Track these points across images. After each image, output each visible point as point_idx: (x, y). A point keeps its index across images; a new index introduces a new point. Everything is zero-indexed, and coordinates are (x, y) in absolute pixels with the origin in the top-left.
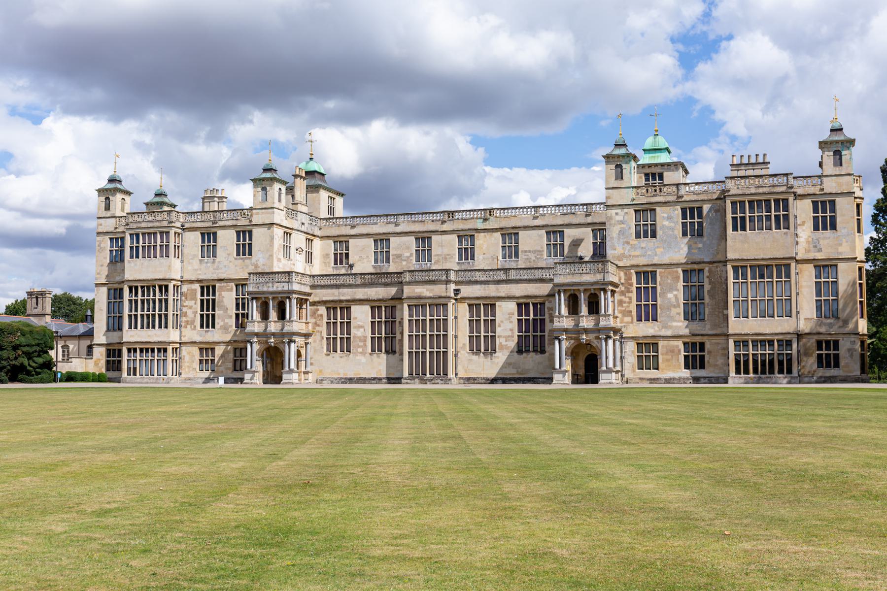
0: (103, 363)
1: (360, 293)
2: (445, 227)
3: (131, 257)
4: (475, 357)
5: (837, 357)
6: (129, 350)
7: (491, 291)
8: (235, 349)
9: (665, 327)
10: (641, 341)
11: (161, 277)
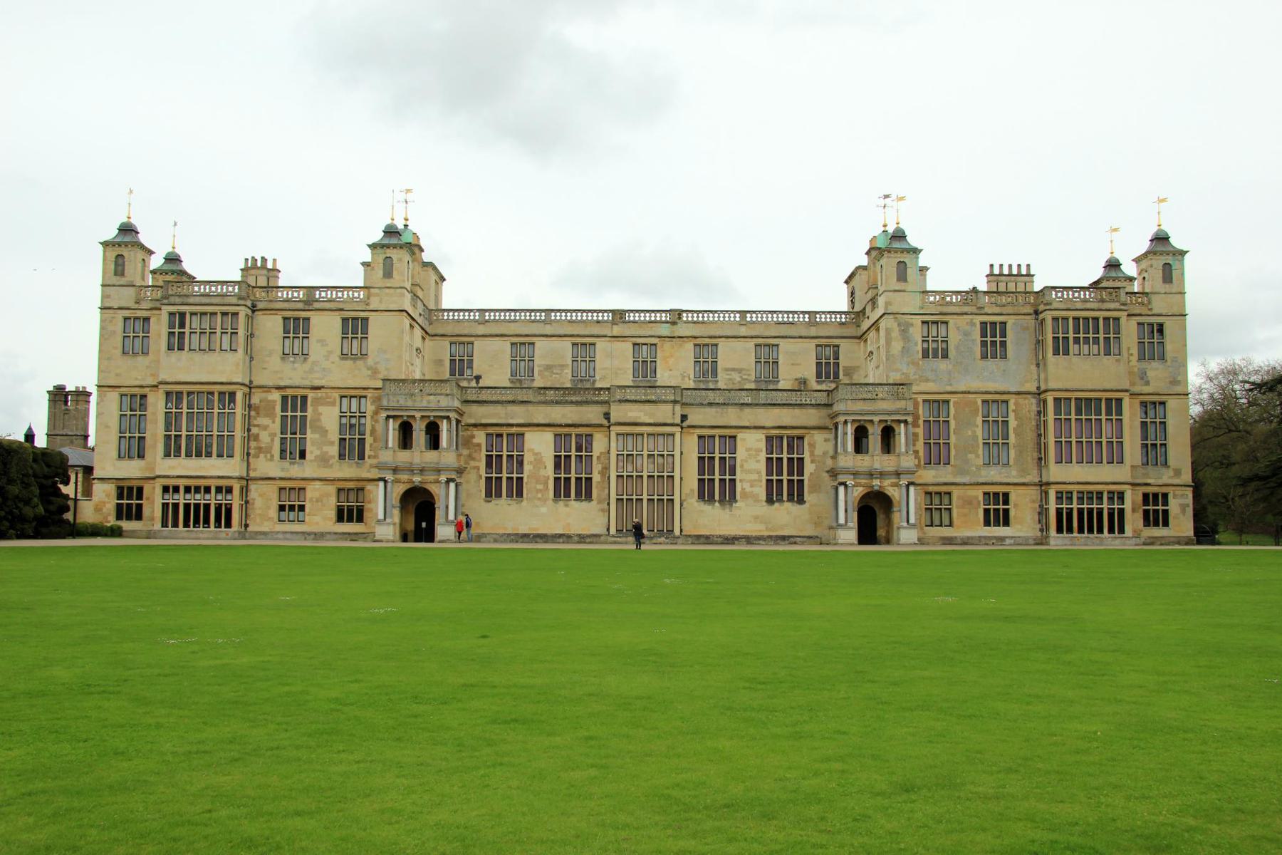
0: (111, 505)
2: (617, 330)
4: (707, 508)
5: (1166, 513)
6: (166, 489)
7: (731, 417)
8: (339, 490)
9: (962, 472)
10: (931, 489)
11: (224, 380)
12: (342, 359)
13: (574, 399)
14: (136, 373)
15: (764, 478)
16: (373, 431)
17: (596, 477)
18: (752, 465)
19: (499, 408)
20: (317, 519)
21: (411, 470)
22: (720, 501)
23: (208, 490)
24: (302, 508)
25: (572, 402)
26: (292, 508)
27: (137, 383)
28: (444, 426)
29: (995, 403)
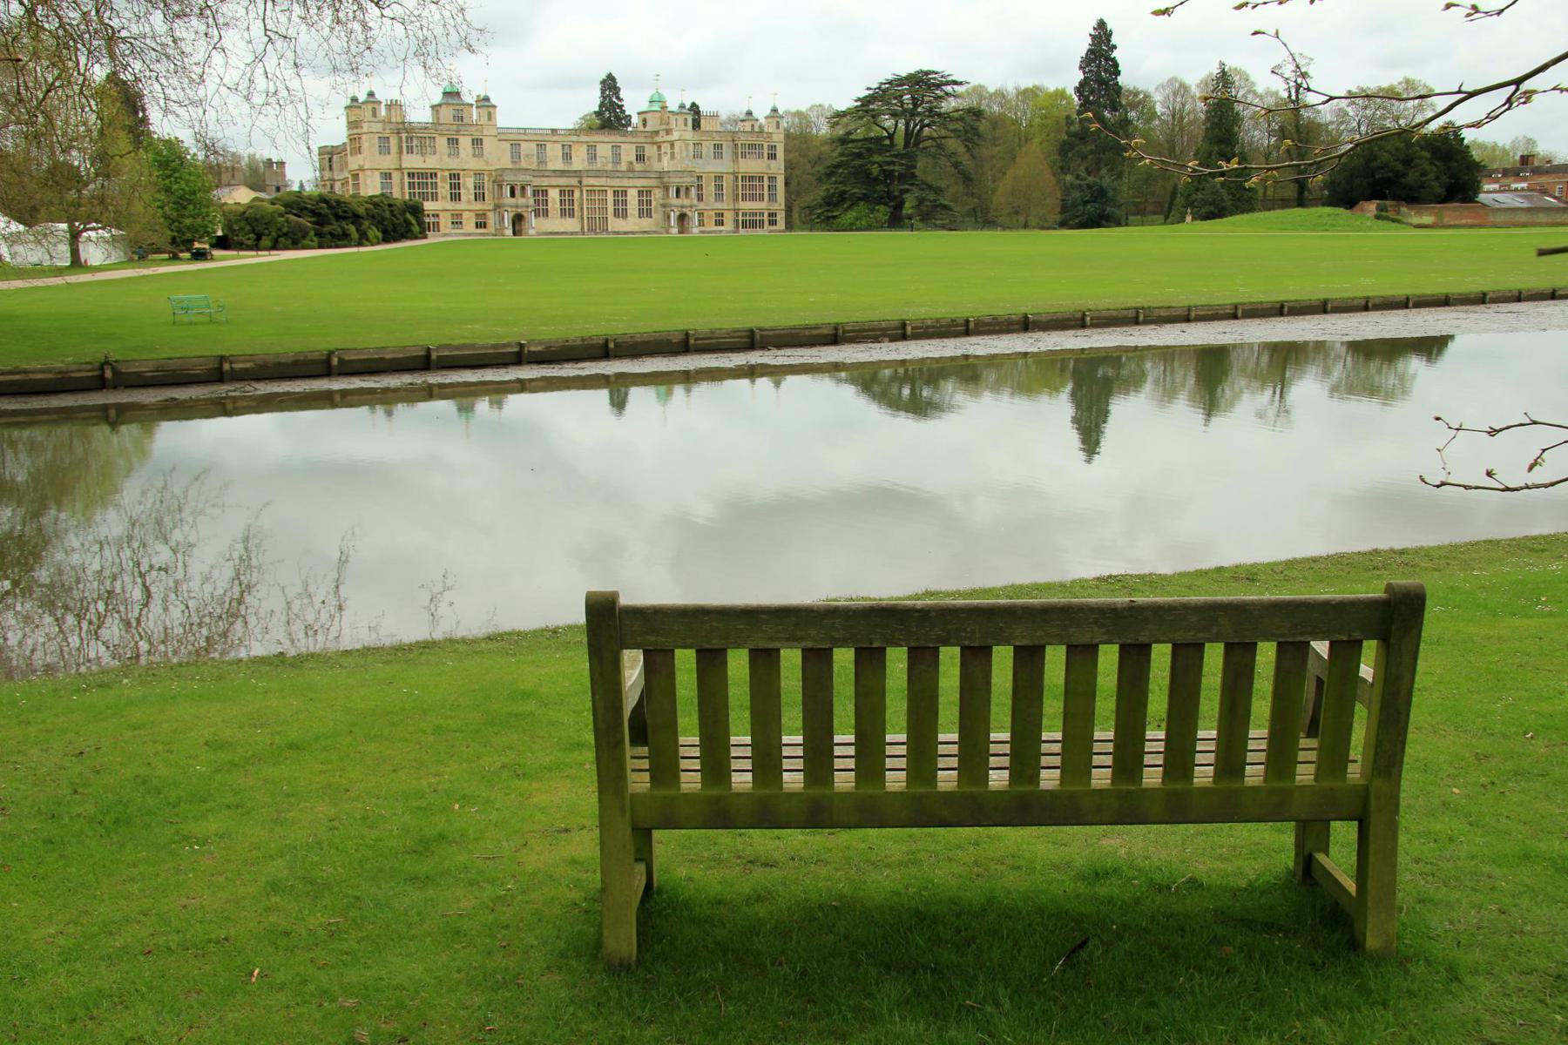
1: (555, 181)
7: (626, 183)
14: (388, 162)
29: (719, 178)
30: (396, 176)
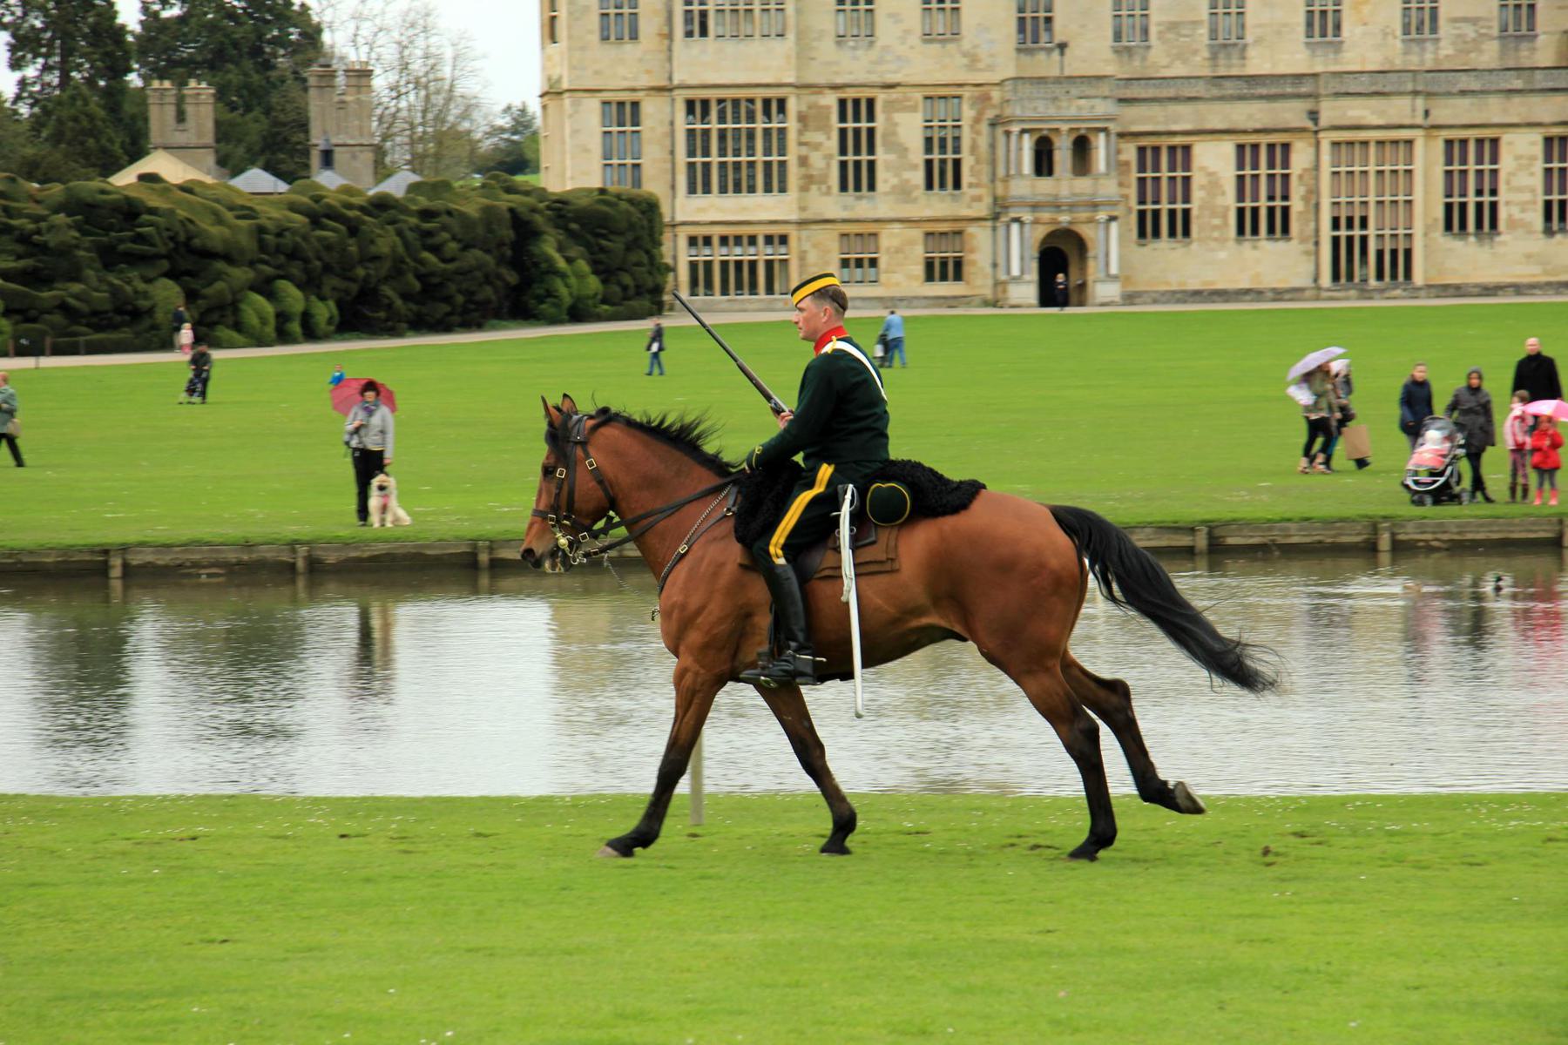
1: (1217, 115)
3: (689, 34)
4: (1456, 244)
6: (693, 241)
7: (1494, 110)
8: (928, 234)
12: (926, 42)
13: (1263, 91)
14: (627, 67)
15: (1541, 198)
16: (974, 148)
17: (1296, 205)
18: (1524, 180)
19: (1155, 111)
20: (897, 277)
21: (1057, 206)
22: (1476, 235)
23: (752, 240)
24: (873, 263)
25: (1261, 97)
26: (859, 263)
27: (626, 84)
28: (1100, 146)
30: (653, 110)
